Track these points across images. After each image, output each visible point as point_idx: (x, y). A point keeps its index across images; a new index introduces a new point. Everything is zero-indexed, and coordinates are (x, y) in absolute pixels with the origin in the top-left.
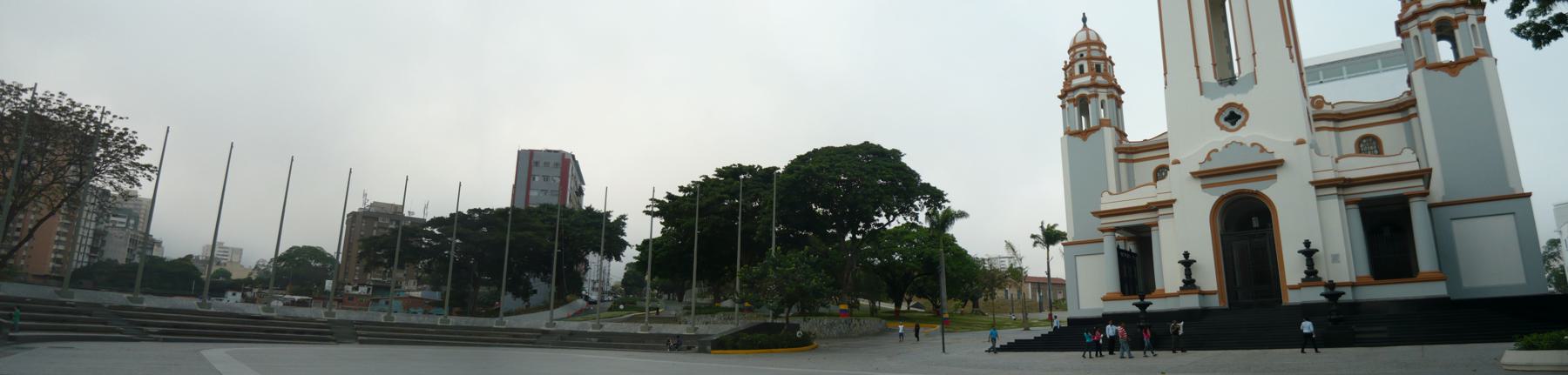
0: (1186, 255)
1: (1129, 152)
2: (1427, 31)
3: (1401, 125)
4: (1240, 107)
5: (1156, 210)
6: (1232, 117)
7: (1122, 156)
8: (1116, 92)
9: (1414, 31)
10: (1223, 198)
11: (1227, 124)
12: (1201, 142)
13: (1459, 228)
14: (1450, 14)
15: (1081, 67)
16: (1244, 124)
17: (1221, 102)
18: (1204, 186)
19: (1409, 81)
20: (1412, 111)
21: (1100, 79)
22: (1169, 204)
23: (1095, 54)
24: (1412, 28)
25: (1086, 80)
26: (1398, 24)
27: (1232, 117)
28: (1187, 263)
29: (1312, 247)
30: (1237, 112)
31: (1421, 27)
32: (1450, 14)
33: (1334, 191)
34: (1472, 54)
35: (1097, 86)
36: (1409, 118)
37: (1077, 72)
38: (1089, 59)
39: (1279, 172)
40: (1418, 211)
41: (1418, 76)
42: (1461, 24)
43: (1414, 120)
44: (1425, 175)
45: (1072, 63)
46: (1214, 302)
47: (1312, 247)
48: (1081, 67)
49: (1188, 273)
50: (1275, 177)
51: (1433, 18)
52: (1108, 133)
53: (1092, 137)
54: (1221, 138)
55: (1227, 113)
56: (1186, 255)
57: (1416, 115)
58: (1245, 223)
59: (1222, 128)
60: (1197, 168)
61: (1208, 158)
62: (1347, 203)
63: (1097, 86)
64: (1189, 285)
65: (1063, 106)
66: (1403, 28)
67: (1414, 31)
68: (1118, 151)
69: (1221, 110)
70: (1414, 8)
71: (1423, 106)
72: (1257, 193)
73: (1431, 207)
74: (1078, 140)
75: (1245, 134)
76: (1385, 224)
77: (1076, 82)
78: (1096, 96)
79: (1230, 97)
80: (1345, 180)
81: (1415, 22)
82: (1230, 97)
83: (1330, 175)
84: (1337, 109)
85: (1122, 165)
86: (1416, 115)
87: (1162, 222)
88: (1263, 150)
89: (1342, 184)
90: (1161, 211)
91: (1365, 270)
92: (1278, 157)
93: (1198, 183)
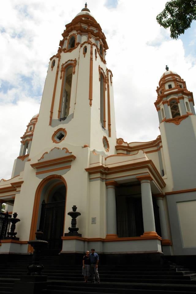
2: (166, 105)
3: (157, 153)
14: (176, 97)
17: (56, 129)
18: (37, 173)
27: (60, 135)
29: (77, 211)
31: (163, 103)
32: (176, 97)
33: (99, 175)
34: (185, 114)
42: (181, 101)
46: (25, 250)
47: (77, 211)
50: (69, 167)
51: (169, 99)
55: (58, 135)
58: (53, 195)
62: (107, 185)
66: (158, 106)
67: (162, 107)
69: (56, 132)
75: (62, 144)
91: (113, 231)
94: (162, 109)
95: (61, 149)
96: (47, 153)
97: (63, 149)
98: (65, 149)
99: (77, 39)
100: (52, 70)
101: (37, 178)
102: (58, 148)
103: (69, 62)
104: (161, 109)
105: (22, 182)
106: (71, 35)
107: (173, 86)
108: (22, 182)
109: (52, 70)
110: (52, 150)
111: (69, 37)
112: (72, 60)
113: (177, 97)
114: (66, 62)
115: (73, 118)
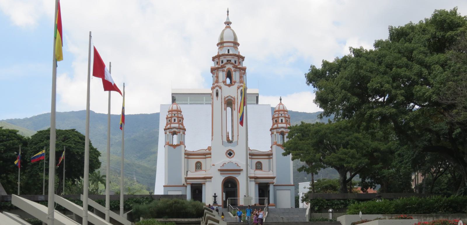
0: (215, 194)
1: (188, 155)
4: (233, 151)
5: (206, 179)
6: (230, 154)
7: (186, 156)
8: (185, 130)
9: (275, 133)
10: (226, 178)
11: (228, 156)
12: (219, 159)
13: (279, 193)
15: (175, 120)
16: (233, 157)
18: (221, 174)
19: (271, 147)
20: (271, 157)
21: (181, 126)
22: (210, 178)
23: (180, 116)
24: (275, 132)
25: (176, 125)
26: (271, 130)
28: (215, 197)
30: (232, 152)
31: (277, 132)
33: (253, 180)
35: (180, 129)
36: (270, 158)
37: (173, 121)
38: (178, 117)
39: (241, 172)
40: (271, 188)
41: (274, 146)
43: (271, 159)
44: (273, 178)
45: (171, 117)
48: (175, 120)
49: (215, 200)
50: (240, 174)
51: (280, 130)
52: (183, 146)
53: (177, 148)
54: (227, 160)
56: (215, 194)
57: (272, 158)
58: (230, 187)
59: (227, 157)
60: (219, 168)
61: (223, 166)
62: (256, 183)
63: (180, 129)
64: (215, 203)
65: (166, 133)
66: (272, 131)
67: (275, 133)
68: (185, 154)
69: (228, 151)
70: (276, 126)
71: (274, 156)
72: (235, 178)
73: (274, 186)
74: (172, 148)
75: (234, 160)
76: (263, 190)
77: (173, 125)
78: (180, 132)
79: (230, 147)
80: (257, 177)
81: (276, 130)
82: (230, 147)
83: (253, 175)
84: (252, 152)
85: (186, 159)
86: (272, 158)
87: (207, 184)
88: (238, 165)
89: (256, 178)
90: (207, 180)
92: (241, 168)
93: (219, 173)
94: (275, 135)
95: (234, 163)
96: (225, 163)
97: (235, 163)
98: (236, 164)
99: (233, 75)
100: (217, 99)
101: (221, 176)
102: (232, 163)
103: (229, 98)
104: (274, 134)
105: (212, 177)
106: (228, 68)
107: (284, 121)
108: (212, 177)
109: (217, 99)
110: (228, 163)
111: (227, 69)
112: (232, 97)
113: (285, 131)
114: (227, 97)
115: (238, 145)
